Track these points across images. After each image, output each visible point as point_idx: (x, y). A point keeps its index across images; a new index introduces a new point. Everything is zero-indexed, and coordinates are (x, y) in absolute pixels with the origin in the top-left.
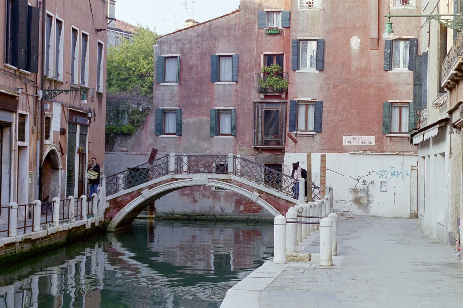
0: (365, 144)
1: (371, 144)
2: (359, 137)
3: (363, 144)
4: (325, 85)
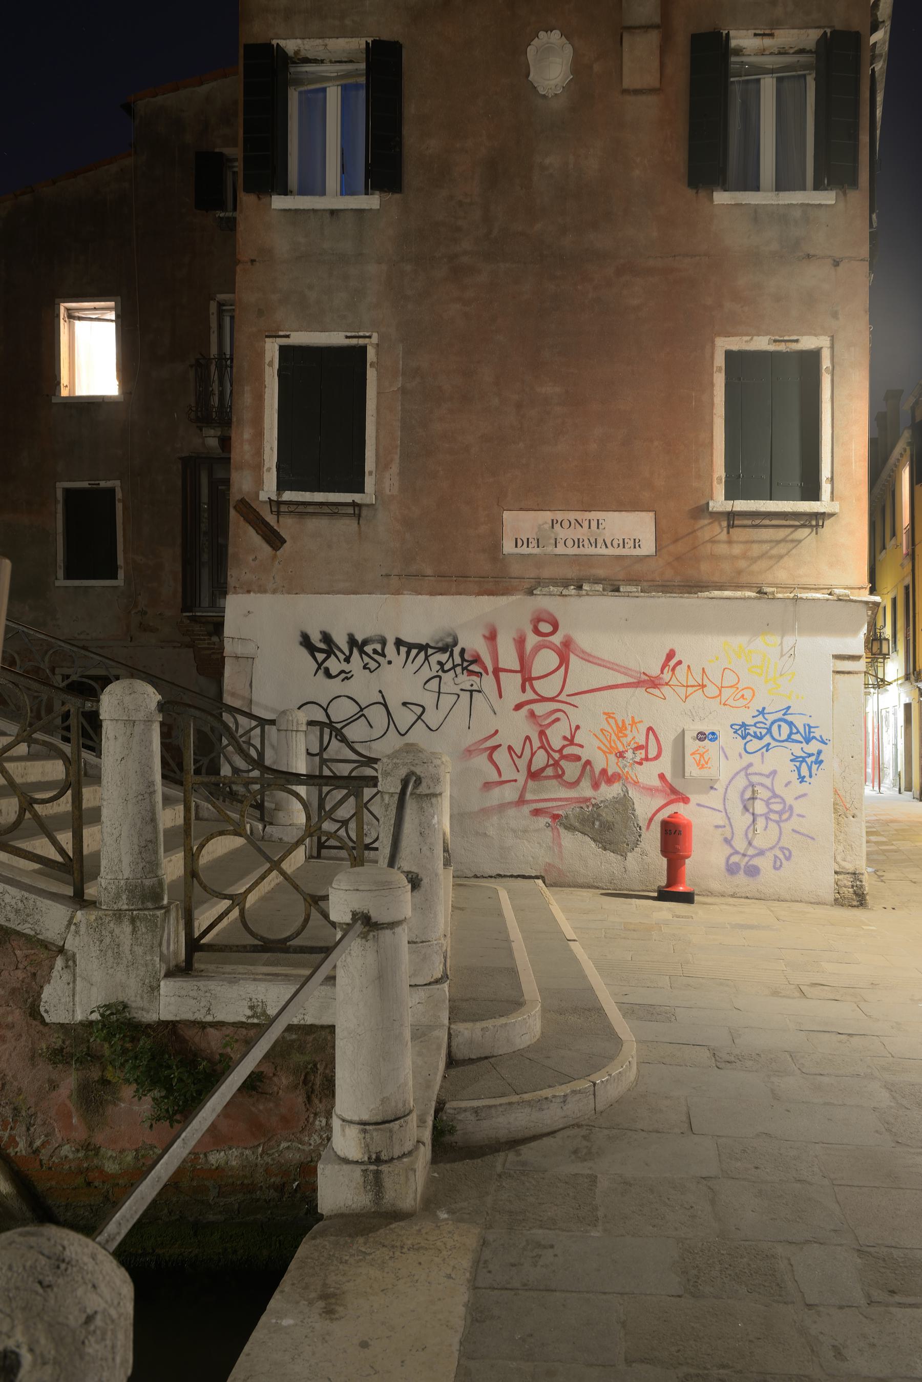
0: (610, 551)
1: (637, 552)
2: (579, 515)
3: (602, 551)
4: (408, 268)
